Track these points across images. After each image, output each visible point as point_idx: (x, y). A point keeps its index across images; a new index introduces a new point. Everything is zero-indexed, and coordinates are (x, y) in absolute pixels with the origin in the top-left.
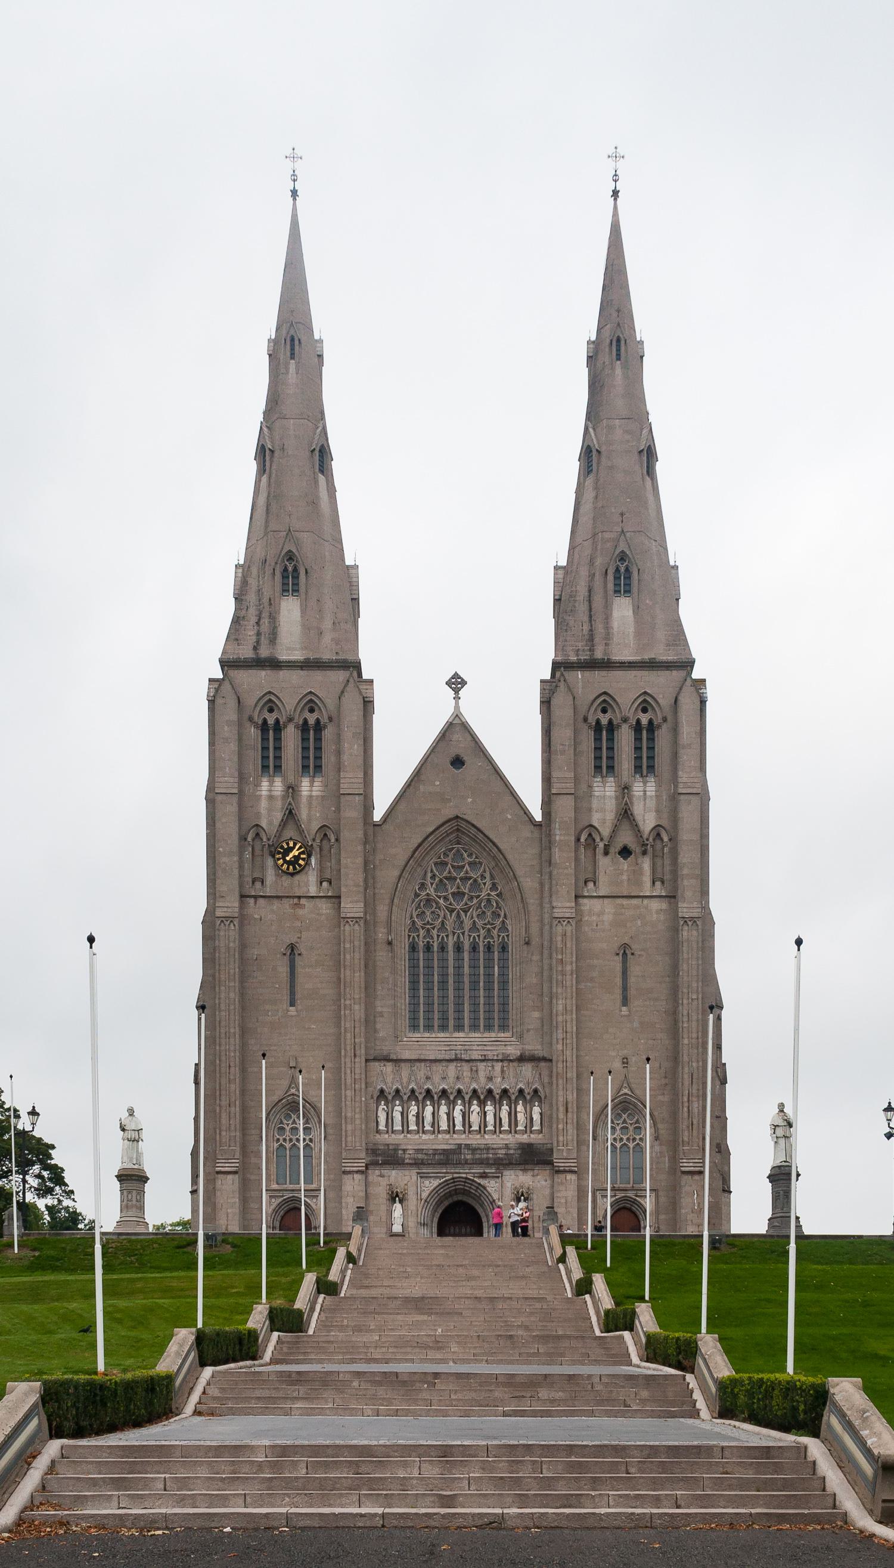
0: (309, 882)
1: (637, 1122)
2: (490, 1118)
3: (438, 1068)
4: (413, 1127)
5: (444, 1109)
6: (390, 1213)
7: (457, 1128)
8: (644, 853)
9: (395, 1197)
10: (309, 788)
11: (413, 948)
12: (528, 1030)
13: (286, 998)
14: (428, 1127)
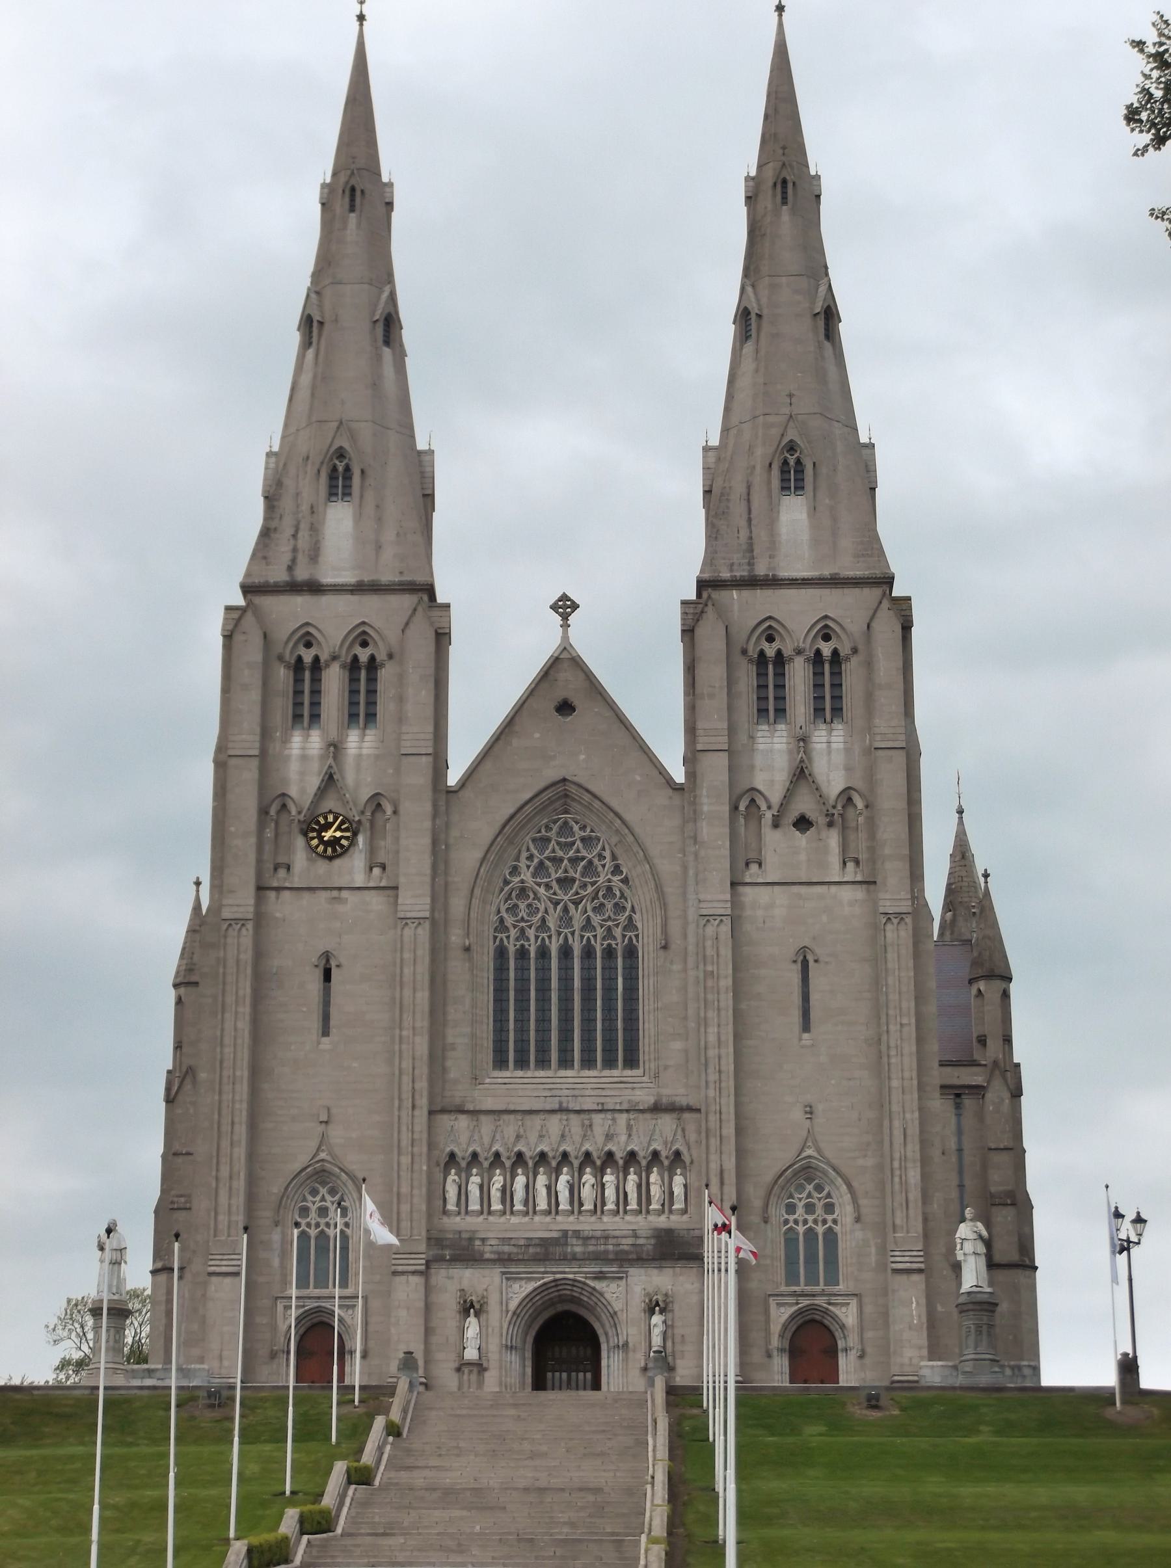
0: (354, 868)
1: (829, 1196)
2: (610, 1192)
3: (537, 1120)
4: (496, 1206)
5: (542, 1180)
6: (462, 1331)
7: (561, 1207)
8: (830, 825)
9: (468, 1308)
10: (359, 744)
11: (501, 953)
12: (666, 1068)
13: (315, 1024)
14: (518, 1207)
